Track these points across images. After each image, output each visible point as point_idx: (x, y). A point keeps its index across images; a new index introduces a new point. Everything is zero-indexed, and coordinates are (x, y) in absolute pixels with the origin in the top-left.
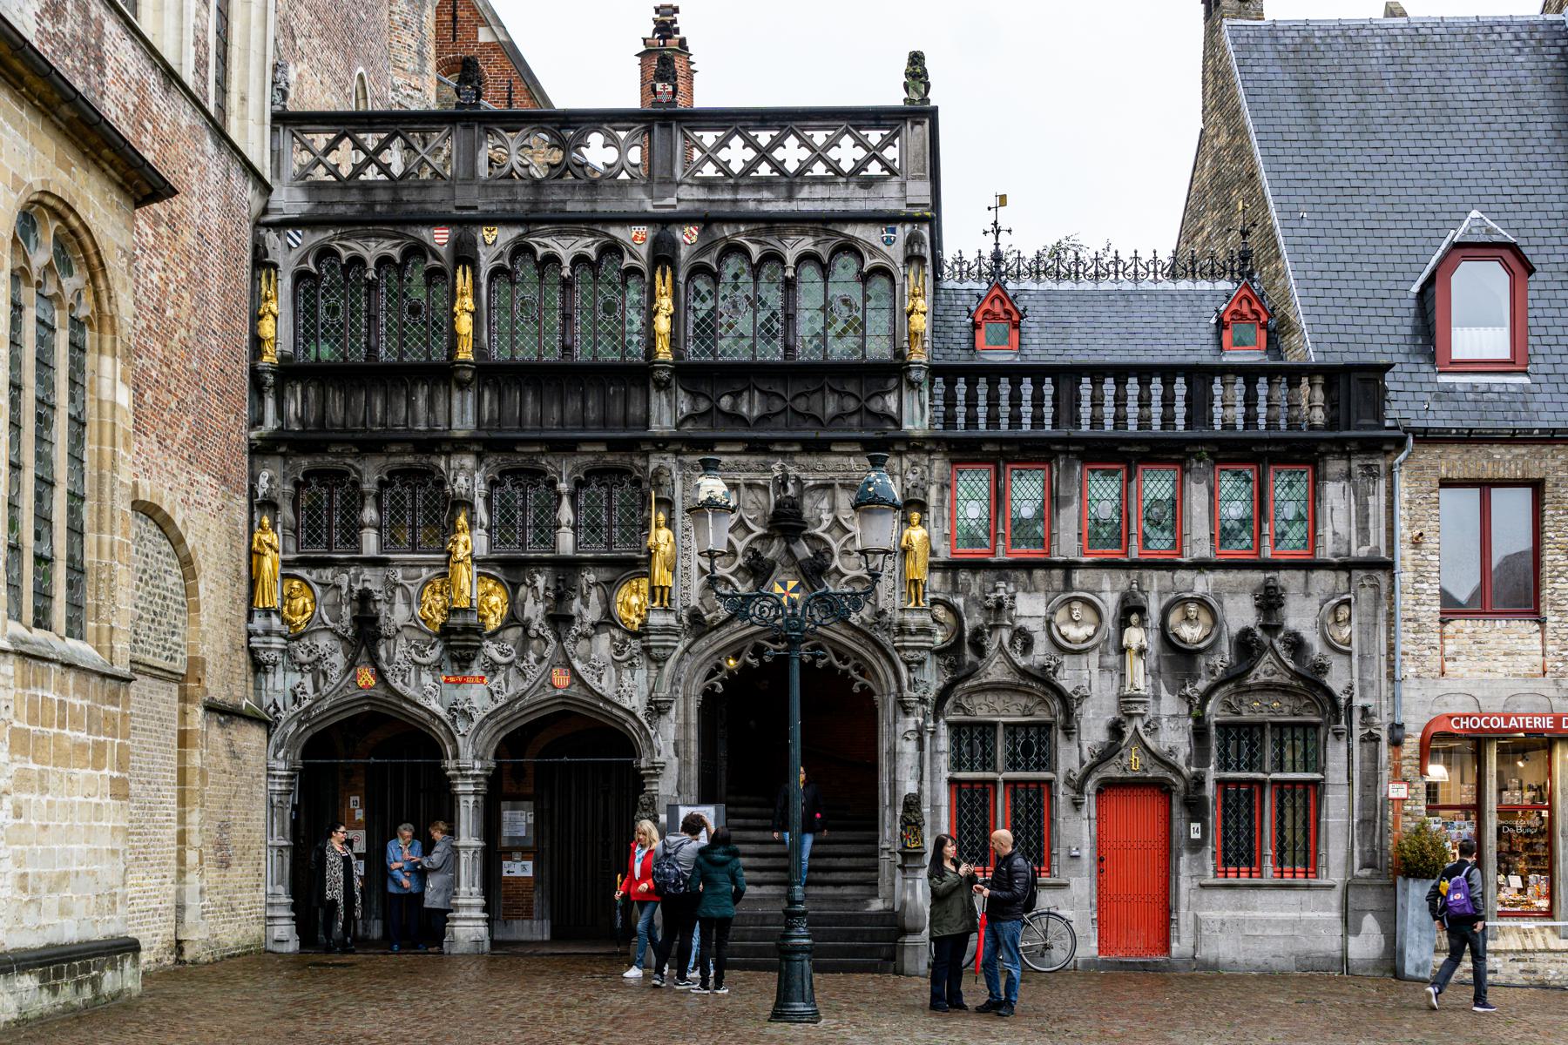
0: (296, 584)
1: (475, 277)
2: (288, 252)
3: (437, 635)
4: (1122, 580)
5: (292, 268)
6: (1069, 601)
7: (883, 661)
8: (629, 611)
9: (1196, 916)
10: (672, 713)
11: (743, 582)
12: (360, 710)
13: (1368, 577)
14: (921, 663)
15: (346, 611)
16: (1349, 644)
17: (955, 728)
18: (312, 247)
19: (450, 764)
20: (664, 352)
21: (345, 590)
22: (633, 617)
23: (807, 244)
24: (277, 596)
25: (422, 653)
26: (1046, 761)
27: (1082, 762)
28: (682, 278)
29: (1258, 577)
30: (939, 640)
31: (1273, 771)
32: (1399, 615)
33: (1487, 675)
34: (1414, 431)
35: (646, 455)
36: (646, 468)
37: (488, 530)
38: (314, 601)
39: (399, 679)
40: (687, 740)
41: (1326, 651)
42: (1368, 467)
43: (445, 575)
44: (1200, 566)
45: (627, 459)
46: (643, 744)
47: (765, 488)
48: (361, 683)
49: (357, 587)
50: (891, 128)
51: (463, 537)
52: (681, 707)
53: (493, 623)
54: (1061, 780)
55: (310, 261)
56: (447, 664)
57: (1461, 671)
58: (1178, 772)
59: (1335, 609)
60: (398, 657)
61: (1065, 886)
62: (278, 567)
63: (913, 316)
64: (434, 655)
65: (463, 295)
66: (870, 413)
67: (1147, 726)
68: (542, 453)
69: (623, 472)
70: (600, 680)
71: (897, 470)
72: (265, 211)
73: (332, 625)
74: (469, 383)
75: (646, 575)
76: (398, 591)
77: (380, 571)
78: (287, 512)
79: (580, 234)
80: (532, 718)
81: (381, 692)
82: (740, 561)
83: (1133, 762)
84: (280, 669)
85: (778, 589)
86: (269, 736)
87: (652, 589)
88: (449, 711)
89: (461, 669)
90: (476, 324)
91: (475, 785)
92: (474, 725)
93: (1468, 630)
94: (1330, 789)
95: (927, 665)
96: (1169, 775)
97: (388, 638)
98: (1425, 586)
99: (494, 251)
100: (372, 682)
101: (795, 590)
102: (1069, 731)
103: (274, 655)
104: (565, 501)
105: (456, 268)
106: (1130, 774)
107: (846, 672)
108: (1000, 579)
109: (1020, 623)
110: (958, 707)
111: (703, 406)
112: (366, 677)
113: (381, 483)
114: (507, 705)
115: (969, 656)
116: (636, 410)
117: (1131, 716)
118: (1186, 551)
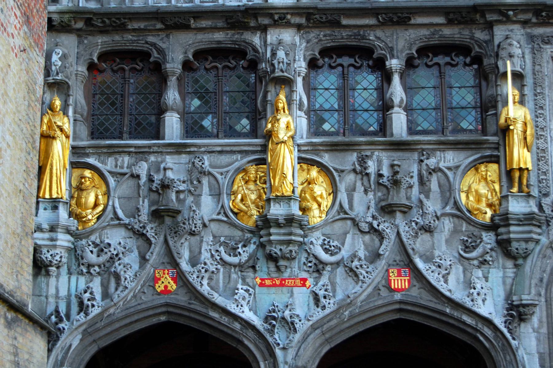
0: (88, 173)
3: (251, 232)
8: (479, 201)
10: (535, 320)
21: (144, 179)
22: (483, 206)
24: (64, 186)
25: (233, 251)
35: (490, 26)
36: (492, 40)
37: (308, 113)
38: (108, 193)
39: (205, 282)
45: (466, 32)
46: (500, 357)
48: (160, 287)
49: (157, 177)
51: (284, 119)
52: (544, 313)
56: (263, 266)
60: (205, 256)
62: (68, 152)
70: (446, 282)
73: (127, 221)
75: (495, 160)
76: (205, 181)
77: (184, 158)
81: (182, 299)
84: (64, 270)
86: (50, 351)
87: (509, 173)
88: (267, 319)
89: (278, 269)
92: (297, 337)
97: (192, 233)
100: (173, 286)
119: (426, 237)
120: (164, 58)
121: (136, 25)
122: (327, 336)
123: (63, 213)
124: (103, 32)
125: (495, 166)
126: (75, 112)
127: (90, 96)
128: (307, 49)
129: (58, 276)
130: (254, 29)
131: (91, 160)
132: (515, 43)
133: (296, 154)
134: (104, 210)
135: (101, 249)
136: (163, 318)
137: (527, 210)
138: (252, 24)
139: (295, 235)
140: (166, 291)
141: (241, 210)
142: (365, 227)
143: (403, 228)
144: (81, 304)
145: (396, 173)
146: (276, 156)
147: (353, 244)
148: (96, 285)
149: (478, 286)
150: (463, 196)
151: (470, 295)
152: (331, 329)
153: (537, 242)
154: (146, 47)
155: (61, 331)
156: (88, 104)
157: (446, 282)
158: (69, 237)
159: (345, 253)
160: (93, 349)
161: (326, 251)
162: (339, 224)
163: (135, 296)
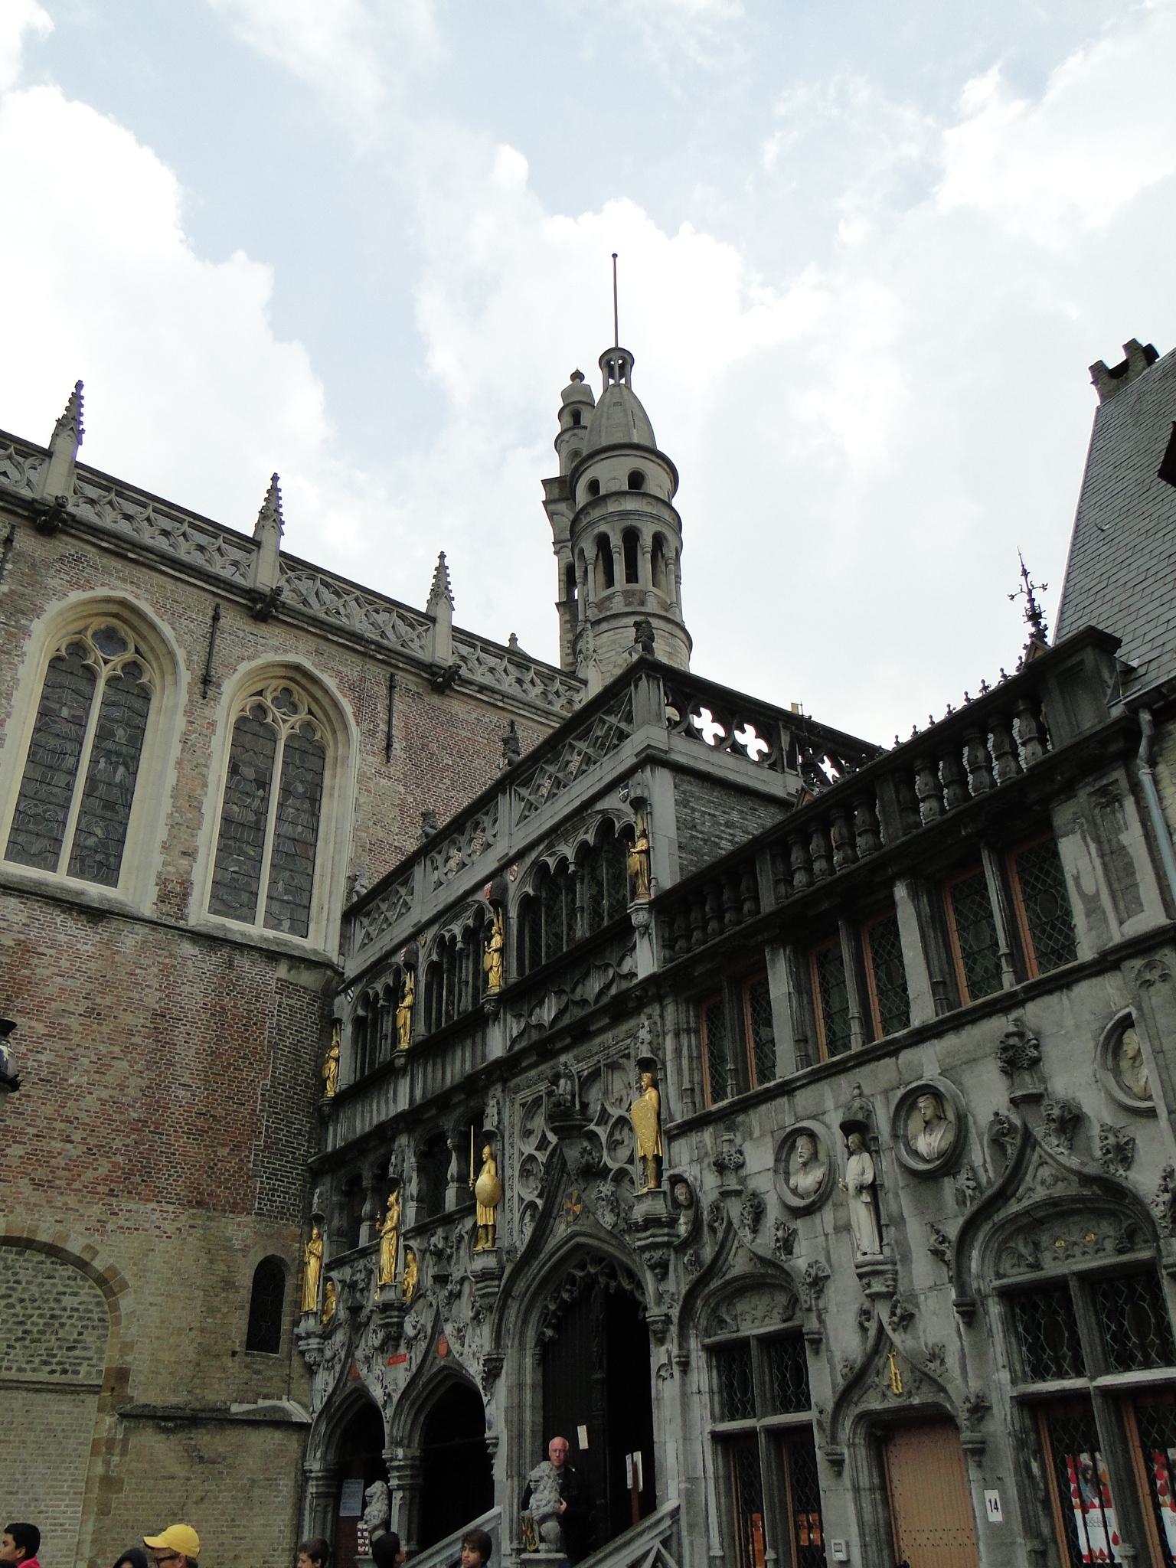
1: (416, 977)
2: (345, 1006)
10: (503, 1372)
13: (1150, 966)
16: (1150, 1098)
30: (683, 1229)
31: (1107, 1372)
40: (520, 1406)
42: (1103, 791)
55: (359, 1009)
64: (381, 1335)
91: (399, 1478)
95: (671, 1268)
96: (940, 1398)
102: (817, 1343)
106: (892, 1403)
107: (632, 1292)
108: (729, 1129)
109: (753, 1184)
111: (523, 1026)
122: (417, 1406)
123: (312, 1321)
128: (416, 1146)
139: (391, 1317)
158: (317, 1340)
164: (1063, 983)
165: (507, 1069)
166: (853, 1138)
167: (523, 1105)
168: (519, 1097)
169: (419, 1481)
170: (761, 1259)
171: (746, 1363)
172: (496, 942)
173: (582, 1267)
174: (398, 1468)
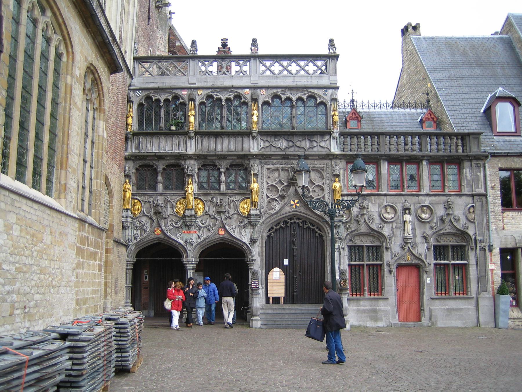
0: (136, 201)
1: (194, 105)
4: (402, 199)
5: (137, 103)
6: (386, 206)
7: (327, 226)
9: (430, 308)
10: (258, 242)
11: (281, 201)
12: (155, 242)
13: (479, 199)
14: (339, 226)
15: (152, 211)
16: (474, 220)
17: (350, 247)
18: (143, 97)
19: (185, 260)
20: (255, 127)
21: (152, 202)
22: (245, 212)
23: (299, 95)
24: (130, 205)
26: (379, 257)
27: (392, 258)
28: (260, 105)
29: (445, 198)
30: (345, 219)
32: (490, 210)
33: (517, 229)
34: (491, 153)
35: (249, 160)
38: (142, 207)
39: (168, 232)
41: (467, 222)
43: (185, 198)
44: (427, 195)
46: (248, 253)
47: (288, 171)
48: (156, 233)
50: (324, 61)
53: (200, 213)
54: (385, 264)
56: (184, 227)
57: (510, 228)
58: (423, 261)
59: (469, 209)
60: (169, 224)
61: (387, 299)
63: (335, 116)
64: (179, 224)
65: (191, 110)
66: (320, 146)
67: (412, 246)
68: (216, 159)
69: (242, 165)
70: (234, 232)
71: (330, 165)
72: (130, 85)
73: (147, 214)
74: (192, 137)
75: (249, 198)
76: (169, 203)
77: (163, 197)
78: (133, 178)
79: (228, 92)
80: (211, 245)
81: (162, 236)
82: (280, 193)
83: (409, 259)
85: (292, 203)
86: (127, 250)
87: (252, 202)
88: (185, 242)
89: (189, 228)
90: (195, 119)
93: (511, 215)
94: (470, 266)
96: (419, 262)
97: (165, 218)
98: (496, 201)
99: (201, 97)
101: (298, 203)
103: (129, 224)
104: (223, 174)
105: (189, 102)
106: (407, 262)
108: (364, 199)
109: (371, 213)
110: (351, 241)
111: (267, 144)
112: (158, 231)
113: (164, 169)
114: (204, 240)
115: (353, 225)
116: (246, 146)
117: (407, 243)
118: (422, 190)
119: (229, 220)
120: (157, 167)
121: (149, 158)
123: (129, 213)
124: (140, 160)
125: (249, 200)
126: (132, 183)
127: (136, 178)
128: (198, 165)
129: (128, 230)
130: (183, 160)
131: (137, 197)
132: (256, 165)
133: (194, 196)
134: (141, 211)
135: (140, 222)
136: (157, 241)
137: (256, 213)
138: (182, 158)
140: (158, 234)
141: (178, 212)
142: (213, 217)
143: (223, 217)
144: (135, 238)
145: (221, 202)
146: (188, 197)
147: (209, 222)
148: (139, 232)
149: (243, 234)
150: (240, 208)
151: (240, 236)
152: (203, 245)
153: (259, 222)
154: (152, 164)
155: (130, 245)
156: (136, 180)
157: (234, 232)
158: (131, 219)
159: (207, 224)
160: (138, 250)
161: (202, 223)
162: (206, 216)
163: (149, 235)
164: (461, 195)
165: (263, 157)
166: (407, 211)
167: (267, 169)
168: (266, 167)
169: (195, 268)
170: (372, 230)
171: (363, 251)
172: (255, 112)
173: (290, 219)
174: (192, 264)
